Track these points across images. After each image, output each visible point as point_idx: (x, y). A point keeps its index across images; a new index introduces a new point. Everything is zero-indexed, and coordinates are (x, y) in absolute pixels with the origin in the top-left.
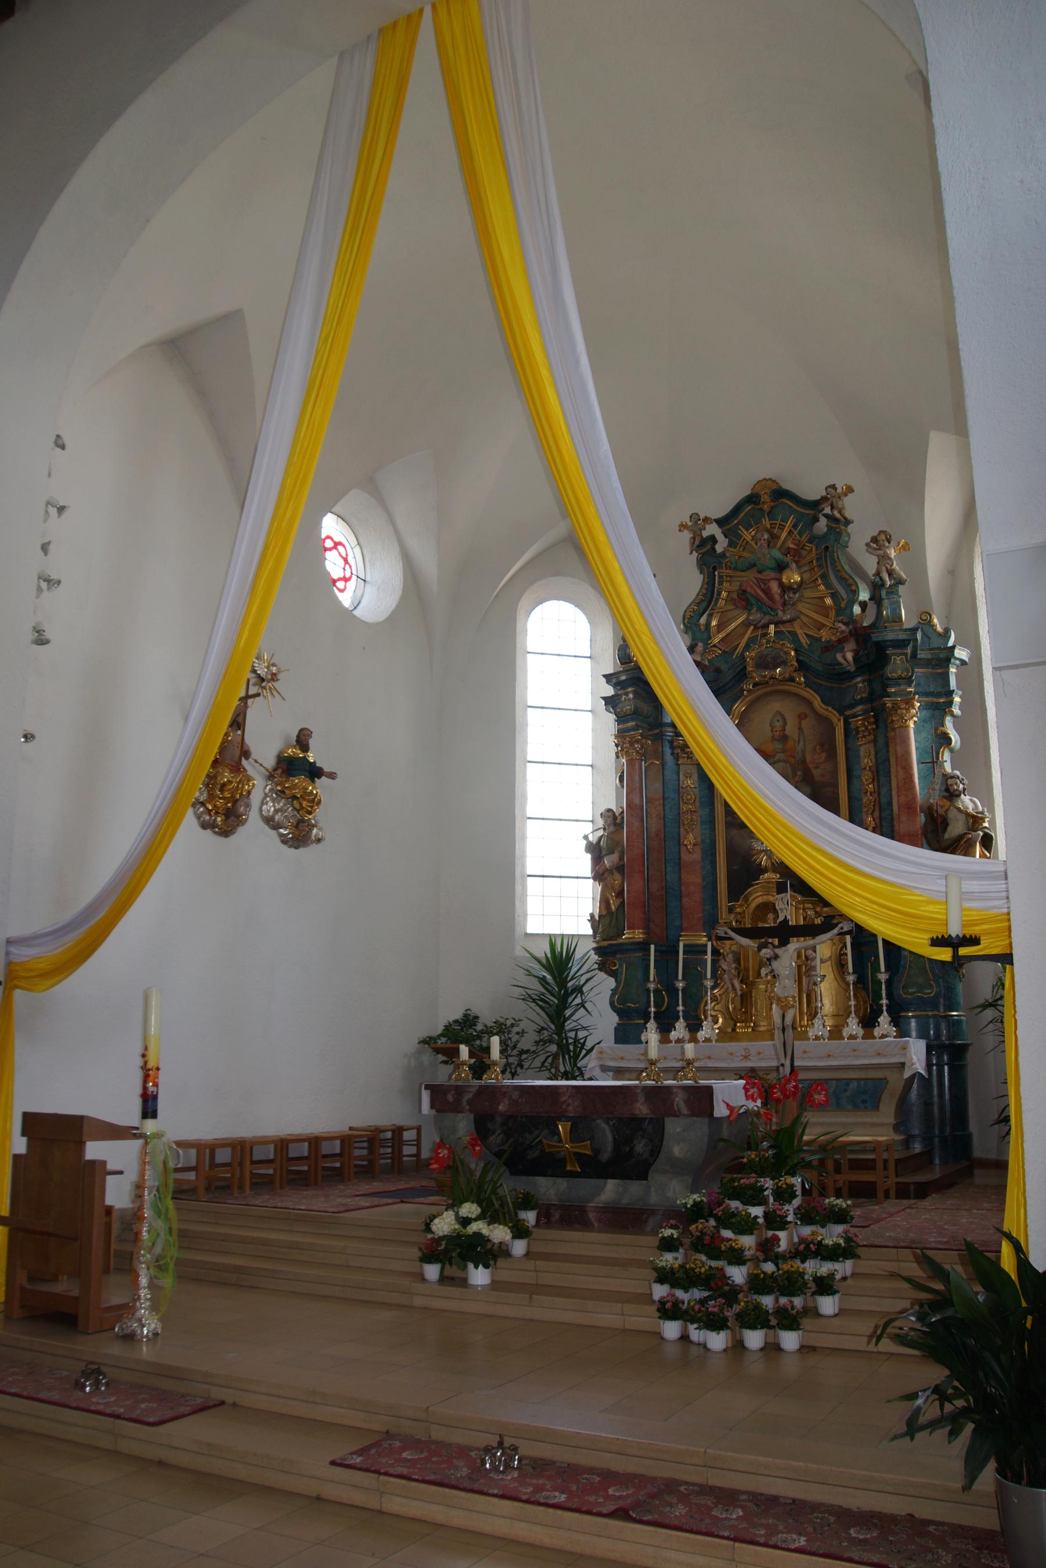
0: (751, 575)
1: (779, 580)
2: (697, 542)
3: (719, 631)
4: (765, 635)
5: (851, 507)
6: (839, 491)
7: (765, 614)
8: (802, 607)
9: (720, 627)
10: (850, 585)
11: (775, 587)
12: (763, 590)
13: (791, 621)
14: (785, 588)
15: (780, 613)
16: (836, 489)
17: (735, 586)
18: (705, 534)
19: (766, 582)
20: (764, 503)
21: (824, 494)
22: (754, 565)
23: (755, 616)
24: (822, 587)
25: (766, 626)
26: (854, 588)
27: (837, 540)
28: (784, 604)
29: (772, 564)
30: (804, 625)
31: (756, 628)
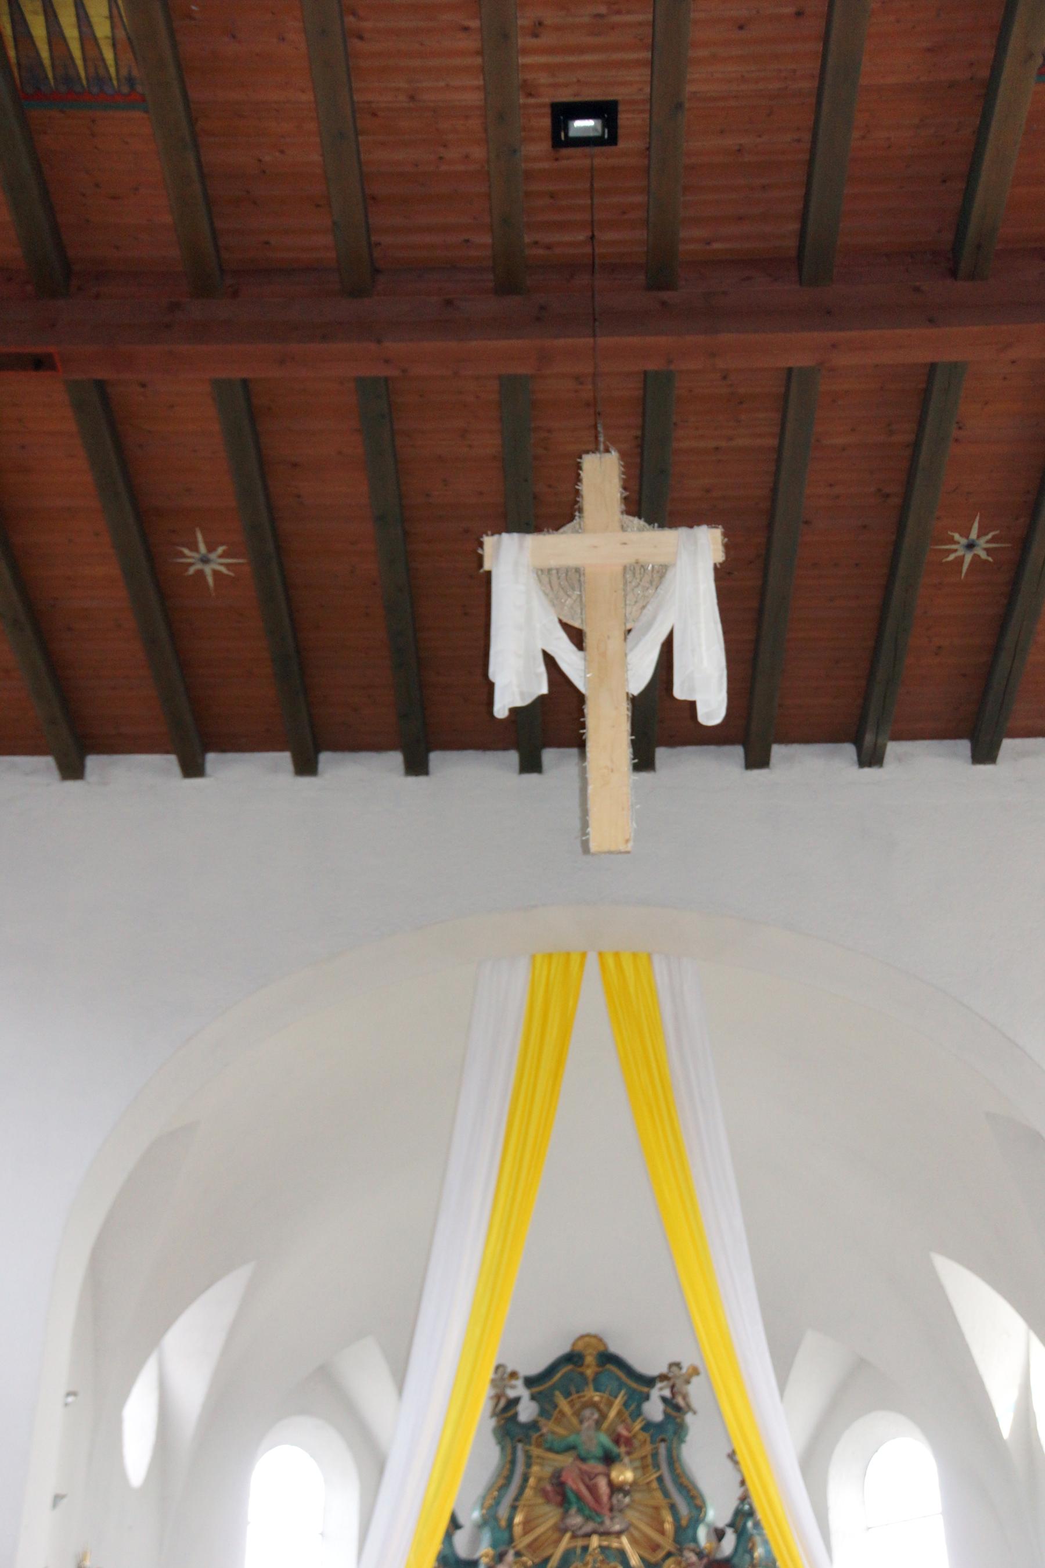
0: (566, 1460)
1: (608, 1476)
2: (503, 1402)
3: (526, 1533)
4: (585, 1549)
5: (695, 1391)
6: (684, 1371)
7: (588, 1519)
8: (632, 1515)
9: (528, 1525)
10: (693, 1498)
11: (602, 1484)
12: (588, 1487)
13: (619, 1534)
14: (615, 1488)
15: (608, 1522)
16: (681, 1368)
17: (548, 1471)
18: (511, 1394)
19: (593, 1476)
20: (588, 1366)
21: (663, 1369)
22: (571, 1448)
23: (576, 1520)
24: (659, 1494)
25: (588, 1535)
26: (698, 1502)
27: (675, 1433)
28: (611, 1510)
29: (599, 1453)
30: (634, 1542)
31: (574, 1536)
